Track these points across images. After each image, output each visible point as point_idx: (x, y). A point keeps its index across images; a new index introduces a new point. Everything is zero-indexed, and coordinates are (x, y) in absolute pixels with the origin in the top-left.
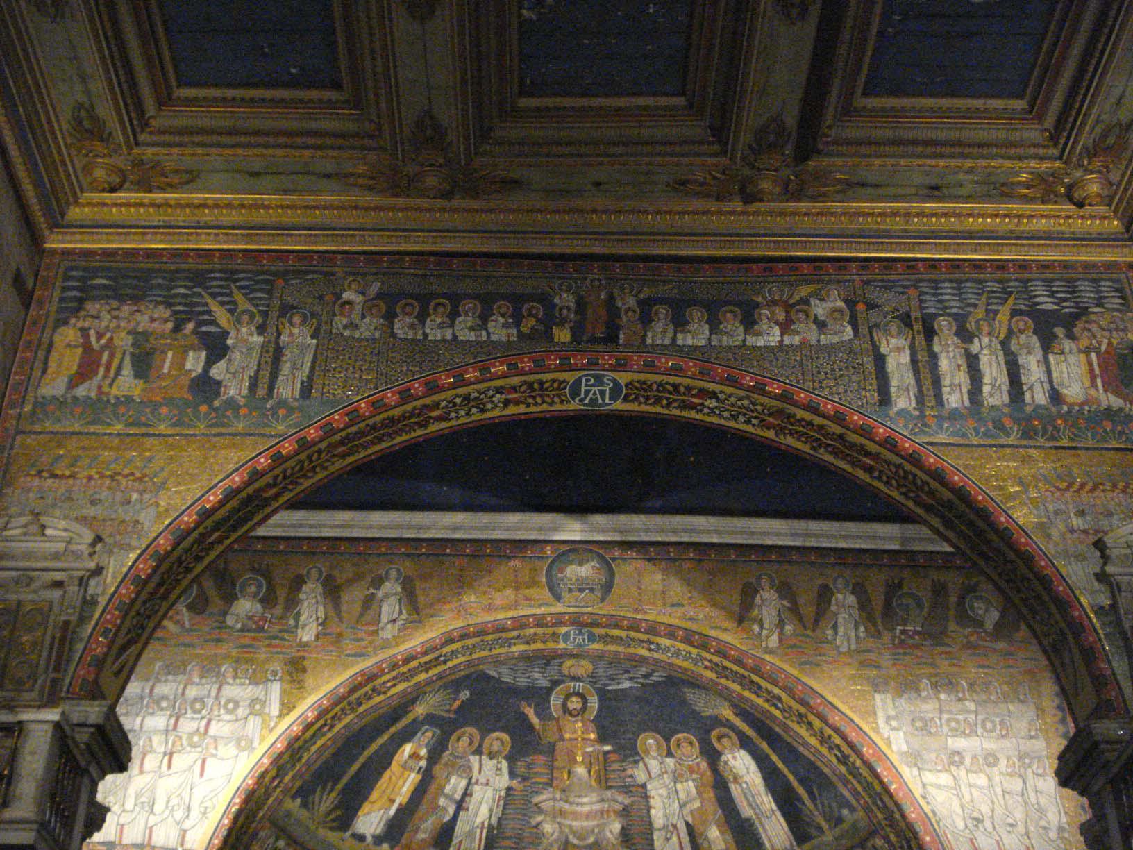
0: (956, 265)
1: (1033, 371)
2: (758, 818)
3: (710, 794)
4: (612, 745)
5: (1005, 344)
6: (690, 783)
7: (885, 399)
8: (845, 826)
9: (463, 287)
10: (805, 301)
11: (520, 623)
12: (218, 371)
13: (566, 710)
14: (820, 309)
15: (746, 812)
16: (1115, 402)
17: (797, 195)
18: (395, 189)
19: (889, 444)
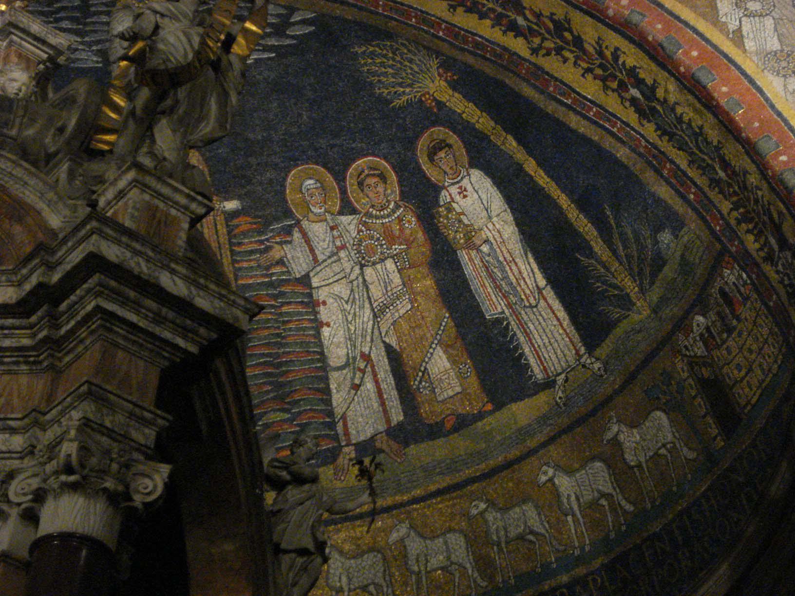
2: (515, 313)
3: (427, 284)
4: (239, 197)
6: (390, 264)
8: (668, 272)
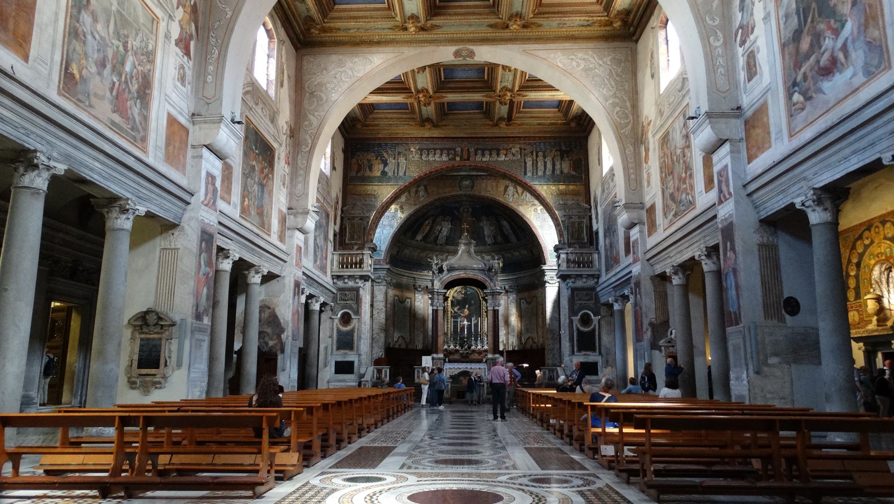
0: (545, 138)
1: (558, 166)
5: (553, 159)
7: (525, 174)
9: (437, 147)
10: (511, 149)
11: (453, 196)
12: (386, 169)
13: (464, 211)
14: (513, 150)
15: (506, 233)
16: (574, 173)
17: (509, 125)
18: (421, 126)
19: (525, 183)
